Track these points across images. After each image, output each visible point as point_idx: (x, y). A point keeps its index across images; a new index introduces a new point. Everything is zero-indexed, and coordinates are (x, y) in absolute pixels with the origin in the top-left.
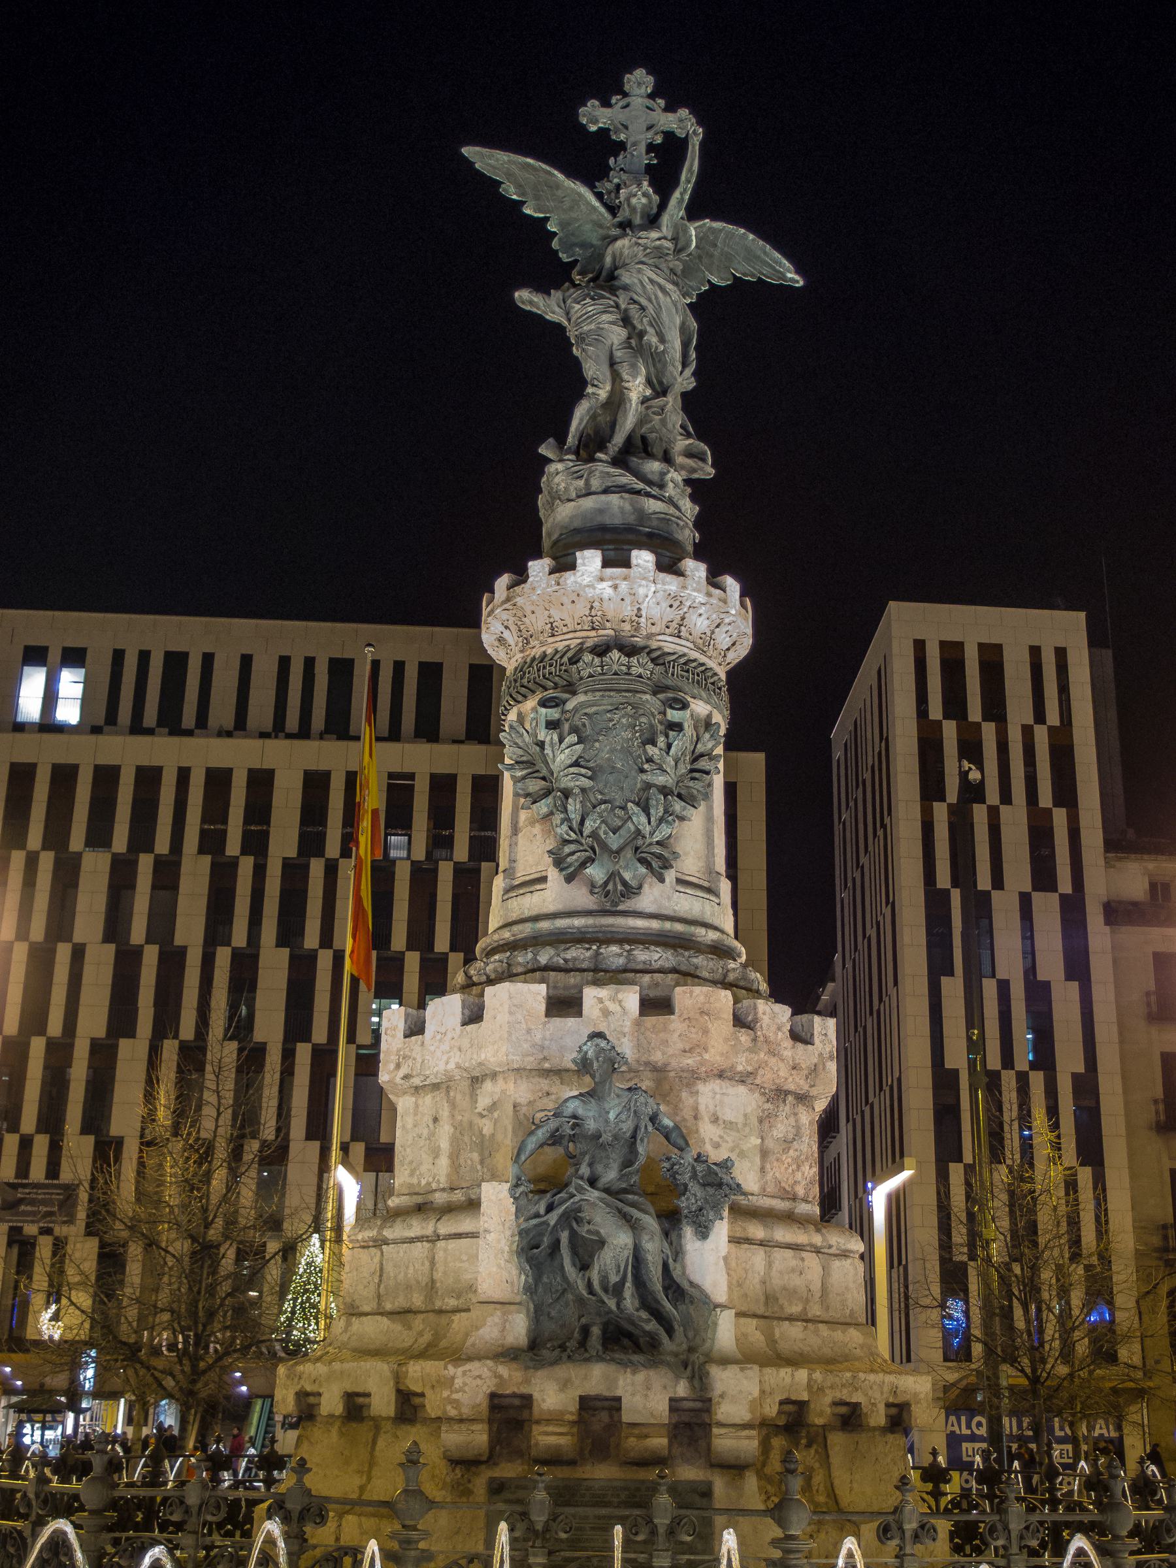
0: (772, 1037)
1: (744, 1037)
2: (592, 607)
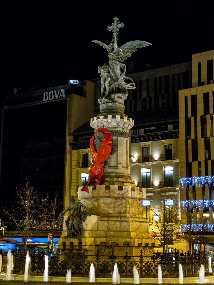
0: (113, 190)
1: (107, 191)
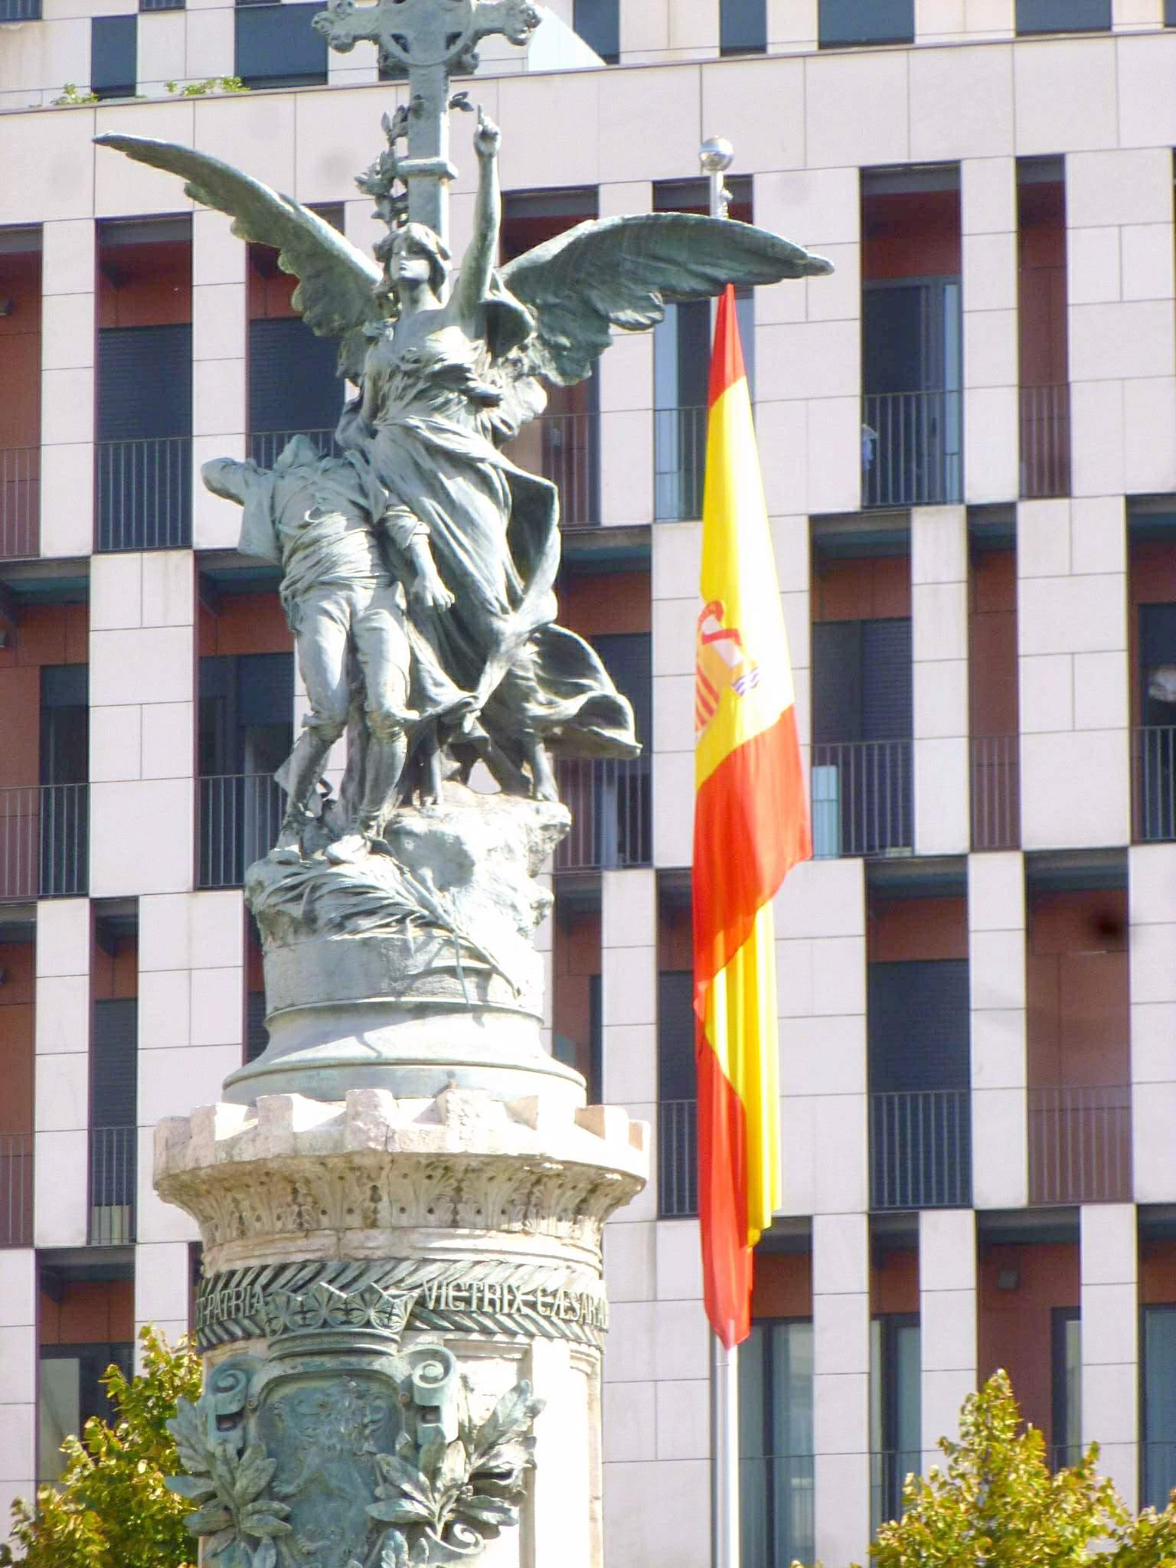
2: (295, 1191)
